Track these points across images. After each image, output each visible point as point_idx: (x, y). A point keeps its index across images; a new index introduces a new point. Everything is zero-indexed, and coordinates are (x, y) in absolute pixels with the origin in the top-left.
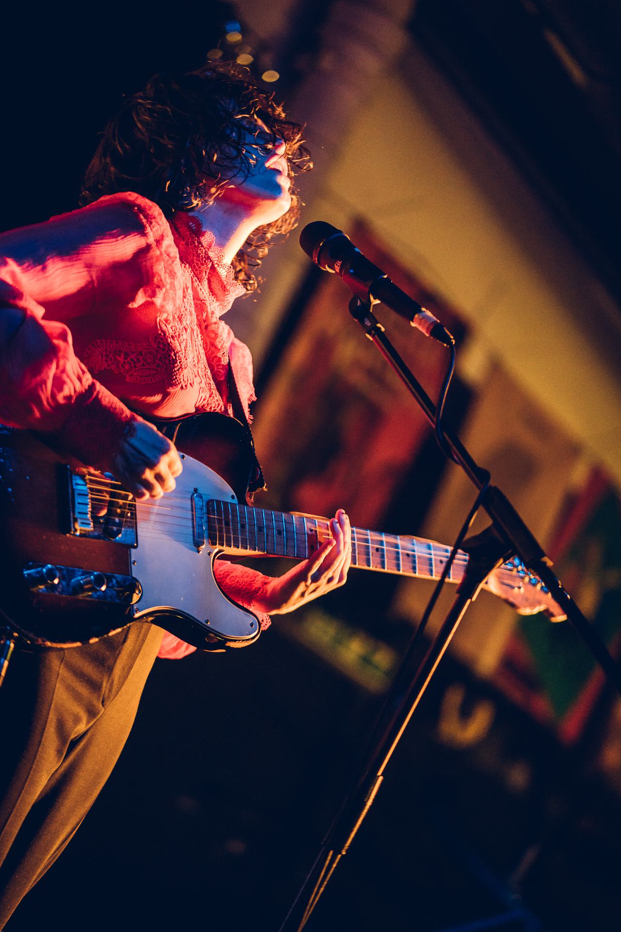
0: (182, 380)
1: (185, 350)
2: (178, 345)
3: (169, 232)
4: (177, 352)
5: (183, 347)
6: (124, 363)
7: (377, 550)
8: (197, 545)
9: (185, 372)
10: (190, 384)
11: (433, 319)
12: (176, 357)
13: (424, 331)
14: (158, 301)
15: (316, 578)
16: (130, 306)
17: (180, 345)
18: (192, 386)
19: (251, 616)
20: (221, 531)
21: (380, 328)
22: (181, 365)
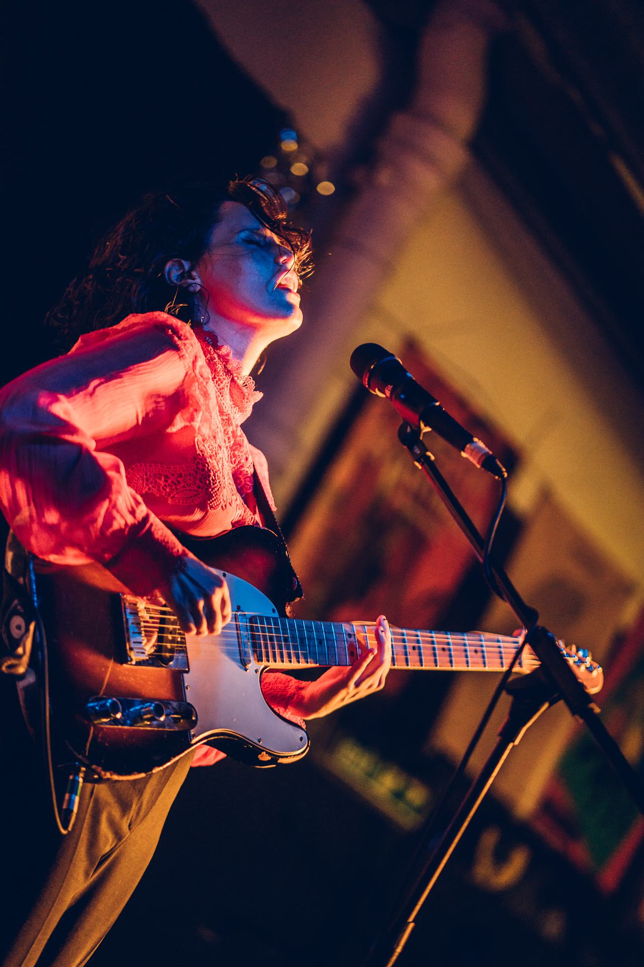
0: (222, 500)
1: (223, 469)
2: (216, 463)
3: (201, 353)
4: (216, 472)
5: (220, 466)
6: (165, 485)
7: (414, 648)
8: (244, 663)
9: (225, 491)
10: (229, 503)
11: (484, 450)
12: (215, 477)
13: (475, 462)
14: (196, 424)
15: (357, 685)
16: (169, 430)
17: (218, 465)
18: (231, 505)
19: (300, 730)
20: (266, 647)
21: (429, 457)
22: (221, 485)
